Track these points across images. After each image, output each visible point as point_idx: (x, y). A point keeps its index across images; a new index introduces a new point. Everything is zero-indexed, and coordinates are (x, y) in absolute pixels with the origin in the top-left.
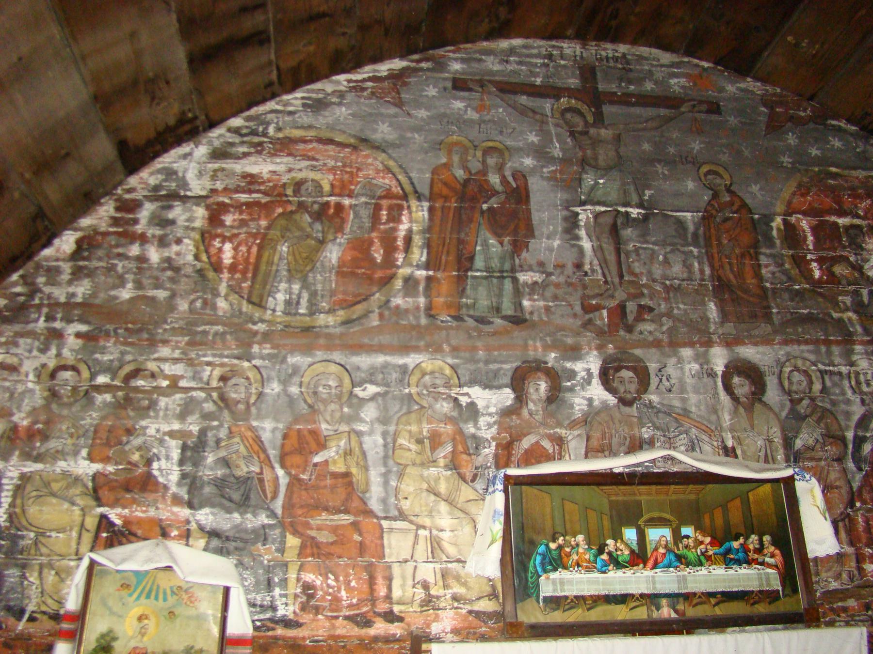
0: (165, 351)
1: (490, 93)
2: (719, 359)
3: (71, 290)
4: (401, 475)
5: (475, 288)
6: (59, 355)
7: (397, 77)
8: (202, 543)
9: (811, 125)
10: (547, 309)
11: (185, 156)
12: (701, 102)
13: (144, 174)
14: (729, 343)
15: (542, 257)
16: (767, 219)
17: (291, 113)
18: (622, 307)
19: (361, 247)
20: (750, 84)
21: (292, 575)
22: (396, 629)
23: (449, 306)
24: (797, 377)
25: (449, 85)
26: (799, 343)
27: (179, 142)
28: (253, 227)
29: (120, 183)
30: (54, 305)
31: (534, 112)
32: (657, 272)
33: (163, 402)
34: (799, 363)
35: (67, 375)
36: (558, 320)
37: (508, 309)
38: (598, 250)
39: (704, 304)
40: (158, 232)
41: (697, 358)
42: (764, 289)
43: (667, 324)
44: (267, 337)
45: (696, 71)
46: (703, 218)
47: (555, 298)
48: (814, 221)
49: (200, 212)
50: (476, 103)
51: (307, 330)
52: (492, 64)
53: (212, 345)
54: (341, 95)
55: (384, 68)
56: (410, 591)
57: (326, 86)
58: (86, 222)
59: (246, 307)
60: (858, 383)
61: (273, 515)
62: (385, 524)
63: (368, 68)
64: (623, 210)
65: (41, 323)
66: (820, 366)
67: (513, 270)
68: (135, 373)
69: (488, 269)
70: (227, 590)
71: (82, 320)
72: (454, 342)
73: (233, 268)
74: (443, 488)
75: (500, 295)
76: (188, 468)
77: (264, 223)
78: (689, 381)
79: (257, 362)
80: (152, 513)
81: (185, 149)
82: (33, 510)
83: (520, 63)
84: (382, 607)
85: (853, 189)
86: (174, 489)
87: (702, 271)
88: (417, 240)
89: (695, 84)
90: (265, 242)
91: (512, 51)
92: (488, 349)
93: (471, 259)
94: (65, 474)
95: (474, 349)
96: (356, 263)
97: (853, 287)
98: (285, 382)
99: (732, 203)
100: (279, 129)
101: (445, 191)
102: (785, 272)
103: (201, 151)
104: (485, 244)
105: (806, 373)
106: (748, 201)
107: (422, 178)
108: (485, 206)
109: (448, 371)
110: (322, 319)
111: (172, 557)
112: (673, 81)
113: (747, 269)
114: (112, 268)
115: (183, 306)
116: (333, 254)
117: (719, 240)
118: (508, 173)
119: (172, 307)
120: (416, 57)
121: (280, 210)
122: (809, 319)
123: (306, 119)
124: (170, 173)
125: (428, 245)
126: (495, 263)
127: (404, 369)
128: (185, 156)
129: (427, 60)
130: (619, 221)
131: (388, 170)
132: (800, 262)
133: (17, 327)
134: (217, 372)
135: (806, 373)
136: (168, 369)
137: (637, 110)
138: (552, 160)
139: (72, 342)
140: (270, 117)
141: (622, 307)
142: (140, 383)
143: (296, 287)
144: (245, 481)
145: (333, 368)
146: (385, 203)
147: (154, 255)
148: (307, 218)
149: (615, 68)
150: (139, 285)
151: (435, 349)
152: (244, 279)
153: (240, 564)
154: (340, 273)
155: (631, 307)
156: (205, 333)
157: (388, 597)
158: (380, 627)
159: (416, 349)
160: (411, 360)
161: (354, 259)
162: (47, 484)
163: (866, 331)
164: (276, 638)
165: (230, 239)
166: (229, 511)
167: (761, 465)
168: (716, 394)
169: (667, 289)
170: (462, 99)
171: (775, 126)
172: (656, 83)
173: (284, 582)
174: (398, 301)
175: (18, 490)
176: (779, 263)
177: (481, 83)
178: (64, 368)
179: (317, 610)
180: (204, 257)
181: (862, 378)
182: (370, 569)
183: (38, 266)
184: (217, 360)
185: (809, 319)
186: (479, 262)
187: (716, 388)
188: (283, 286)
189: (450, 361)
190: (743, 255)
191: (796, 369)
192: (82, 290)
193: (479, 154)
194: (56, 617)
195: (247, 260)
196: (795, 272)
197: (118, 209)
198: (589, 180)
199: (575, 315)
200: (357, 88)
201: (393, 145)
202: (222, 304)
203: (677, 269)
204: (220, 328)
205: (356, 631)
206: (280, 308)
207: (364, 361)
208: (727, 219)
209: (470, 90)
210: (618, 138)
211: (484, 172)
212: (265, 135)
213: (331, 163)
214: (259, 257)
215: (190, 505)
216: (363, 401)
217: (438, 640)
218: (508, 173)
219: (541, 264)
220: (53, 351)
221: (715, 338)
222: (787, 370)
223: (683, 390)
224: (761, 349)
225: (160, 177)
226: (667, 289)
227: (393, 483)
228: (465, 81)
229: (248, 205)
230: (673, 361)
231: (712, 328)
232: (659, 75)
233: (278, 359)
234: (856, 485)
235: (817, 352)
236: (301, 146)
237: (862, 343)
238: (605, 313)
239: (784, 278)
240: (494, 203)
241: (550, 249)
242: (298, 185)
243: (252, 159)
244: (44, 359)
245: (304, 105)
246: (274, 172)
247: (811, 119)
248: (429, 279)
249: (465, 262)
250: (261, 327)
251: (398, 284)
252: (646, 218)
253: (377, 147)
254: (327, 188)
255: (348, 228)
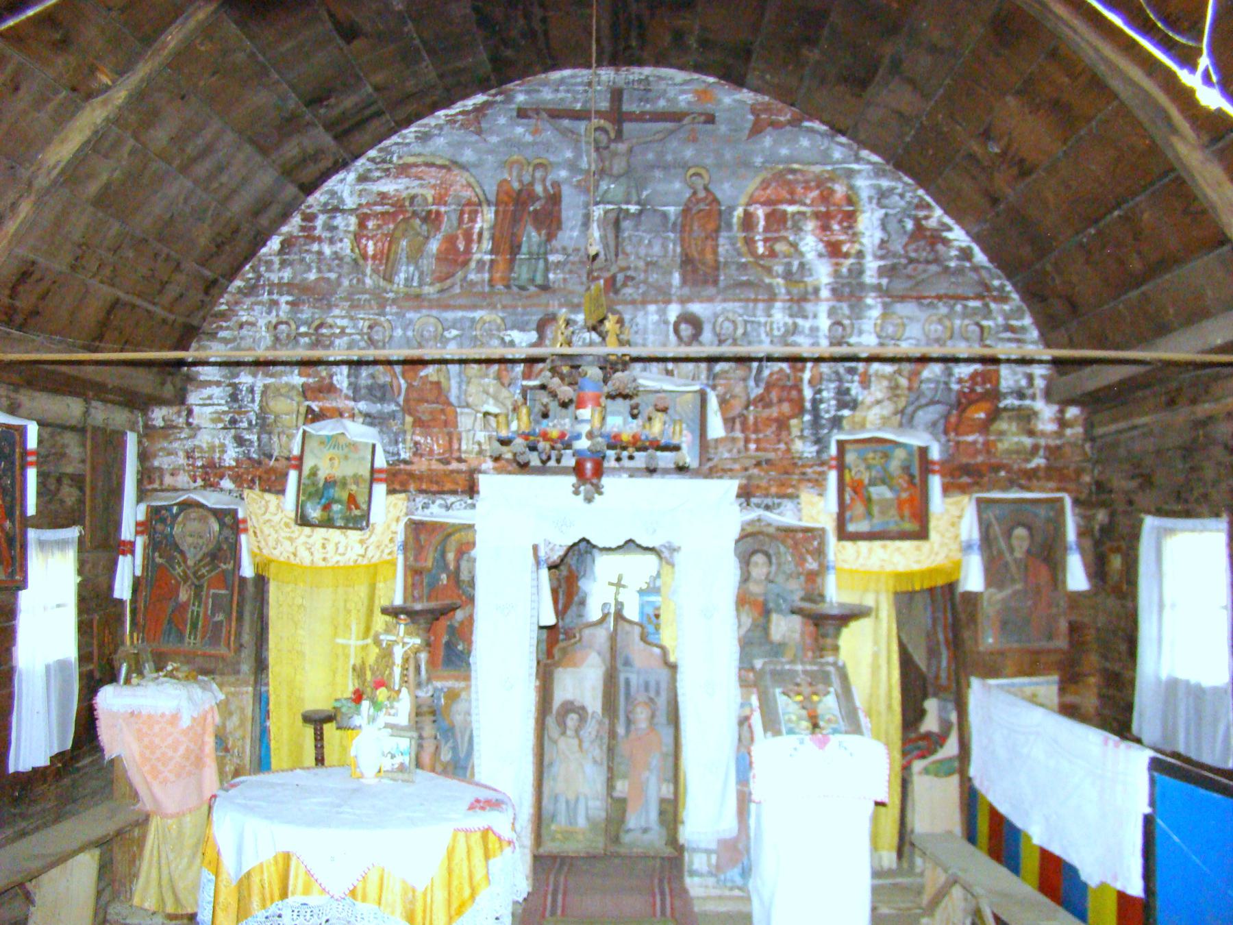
0: (337, 312)
1: (542, 119)
2: (673, 312)
3: (281, 274)
4: (468, 383)
5: (520, 266)
6: (277, 315)
7: (480, 110)
8: (361, 420)
9: (788, 128)
10: (565, 280)
11: (342, 181)
12: (701, 114)
13: (317, 195)
14: (683, 301)
15: (566, 243)
16: (731, 209)
17: (408, 144)
18: (614, 278)
19: (451, 240)
20: (746, 96)
21: (408, 437)
22: (463, 467)
23: (503, 279)
24: (727, 324)
25: (515, 114)
26: (734, 301)
27: (337, 172)
28: (385, 229)
29: (303, 202)
30: (272, 285)
31: (573, 132)
32: (642, 251)
33: (337, 342)
34: (731, 316)
35: (283, 327)
36: (570, 287)
37: (539, 280)
38: (604, 238)
39: (671, 273)
40: (328, 235)
41: (658, 312)
42: (717, 261)
43: (642, 288)
44: (394, 301)
45: (703, 86)
46: (683, 210)
47: (571, 272)
48: (768, 209)
49: (353, 220)
50: (532, 129)
51: (418, 297)
52: (547, 95)
53: (363, 307)
54: (440, 127)
55: (470, 103)
56: (471, 447)
57: (430, 121)
58: (285, 229)
59: (382, 283)
60: (772, 329)
61: (398, 404)
62: (459, 410)
63: (460, 104)
64: (624, 207)
65: (266, 297)
66: (746, 318)
67: (546, 253)
68: (321, 325)
69: (530, 253)
70: (374, 446)
71: (289, 293)
72: (505, 302)
73: (374, 257)
74: (491, 390)
75: (535, 271)
76: (353, 379)
77: (392, 226)
78: (650, 327)
79: (389, 317)
80: (334, 404)
81: (340, 175)
82: (272, 404)
83: (568, 91)
84: (456, 455)
85: (807, 182)
86: (345, 391)
87: (674, 251)
88: (486, 235)
89: (699, 99)
90: (392, 239)
91: (562, 81)
92: (524, 307)
93: (519, 247)
94: (287, 384)
95: (515, 307)
96: (447, 251)
97: (786, 260)
98: (405, 329)
99: (706, 198)
100: (400, 158)
101: (506, 199)
102: (736, 250)
103: (351, 177)
104: (529, 237)
105: (733, 322)
106: (719, 196)
107: (491, 190)
108: (531, 209)
109: (499, 321)
110: (427, 289)
111: (345, 428)
112: (682, 98)
113: (708, 250)
114: (302, 260)
115: (346, 283)
116: (434, 246)
117: (691, 226)
118: (548, 184)
119: (339, 284)
120: (493, 91)
121: (401, 217)
122: (748, 284)
123: (416, 148)
124: (333, 194)
125: (493, 238)
126: (535, 249)
127: (473, 320)
128: (342, 181)
129: (500, 93)
130: (622, 216)
131: (469, 185)
132: (749, 242)
133: (253, 299)
134: (367, 324)
135: (733, 322)
136: (339, 322)
137: (648, 125)
138: (580, 171)
139: (284, 308)
140: (394, 148)
141: (614, 278)
142: (324, 331)
143: (411, 269)
144: (383, 387)
145: (432, 320)
146: (467, 209)
147: (327, 250)
148: (418, 222)
149: (638, 90)
150: (319, 270)
151: (492, 307)
152: (381, 263)
153: (381, 432)
154: (438, 259)
155: (620, 277)
156: (359, 300)
157: (459, 449)
158: (454, 465)
159: (482, 308)
160: (477, 314)
161: (446, 249)
162: (278, 390)
163: (789, 293)
164: (400, 470)
165: (372, 238)
166: (374, 403)
167: (689, 381)
168: (667, 336)
169: (648, 264)
170: (523, 125)
171: (757, 130)
172: (668, 100)
173: (404, 441)
174: (472, 276)
175: (264, 393)
176: (733, 242)
177: (537, 111)
178: (282, 323)
179: (421, 456)
180: (357, 250)
181: (775, 326)
182: (450, 435)
183: (260, 260)
184: (366, 316)
185: (748, 284)
186: (524, 249)
187: (668, 331)
188: (404, 268)
189: (501, 314)
190: (707, 238)
191: (727, 319)
192: (287, 274)
193: (531, 169)
194: (288, 459)
195: (382, 252)
196: (744, 249)
197: (303, 220)
198: (603, 186)
199: (582, 283)
200: (451, 121)
201: (475, 166)
202: (368, 281)
203: (657, 249)
204: (367, 296)
205: (441, 467)
206: (402, 282)
207: (450, 315)
208: (700, 211)
209: (529, 117)
210: (631, 150)
211: (532, 184)
212: (391, 162)
213: (433, 181)
214: (389, 250)
215: (355, 400)
216: (448, 340)
217: (485, 472)
218: (548, 184)
219: (564, 249)
220: (274, 313)
221: (674, 298)
222: (721, 319)
223: (645, 331)
224: (705, 305)
225: (327, 196)
226: (648, 264)
227: (464, 387)
228: (526, 110)
229: (383, 214)
230: (641, 314)
231: (674, 290)
232: (672, 93)
233: (400, 315)
234: (752, 396)
235: (745, 308)
236: (414, 170)
237: (784, 301)
238: (602, 282)
239: (735, 254)
240: (538, 206)
241: (571, 238)
242: (413, 198)
243: (383, 181)
244: (269, 318)
245: (417, 138)
246: (397, 190)
247: (790, 123)
248: (492, 261)
249: (515, 249)
250: (391, 295)
251: (473, 265)
252: (641, 212)
253: (463, 167)
254: (430, 200)
255: (443, 227)
